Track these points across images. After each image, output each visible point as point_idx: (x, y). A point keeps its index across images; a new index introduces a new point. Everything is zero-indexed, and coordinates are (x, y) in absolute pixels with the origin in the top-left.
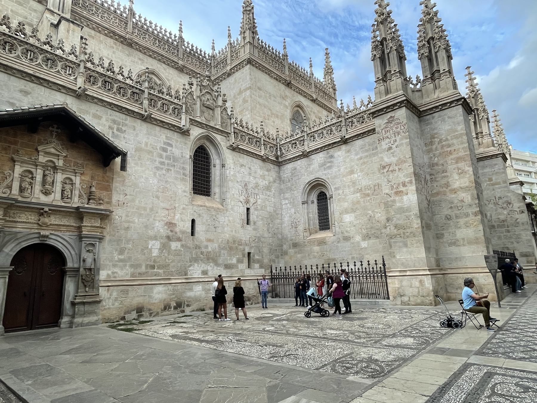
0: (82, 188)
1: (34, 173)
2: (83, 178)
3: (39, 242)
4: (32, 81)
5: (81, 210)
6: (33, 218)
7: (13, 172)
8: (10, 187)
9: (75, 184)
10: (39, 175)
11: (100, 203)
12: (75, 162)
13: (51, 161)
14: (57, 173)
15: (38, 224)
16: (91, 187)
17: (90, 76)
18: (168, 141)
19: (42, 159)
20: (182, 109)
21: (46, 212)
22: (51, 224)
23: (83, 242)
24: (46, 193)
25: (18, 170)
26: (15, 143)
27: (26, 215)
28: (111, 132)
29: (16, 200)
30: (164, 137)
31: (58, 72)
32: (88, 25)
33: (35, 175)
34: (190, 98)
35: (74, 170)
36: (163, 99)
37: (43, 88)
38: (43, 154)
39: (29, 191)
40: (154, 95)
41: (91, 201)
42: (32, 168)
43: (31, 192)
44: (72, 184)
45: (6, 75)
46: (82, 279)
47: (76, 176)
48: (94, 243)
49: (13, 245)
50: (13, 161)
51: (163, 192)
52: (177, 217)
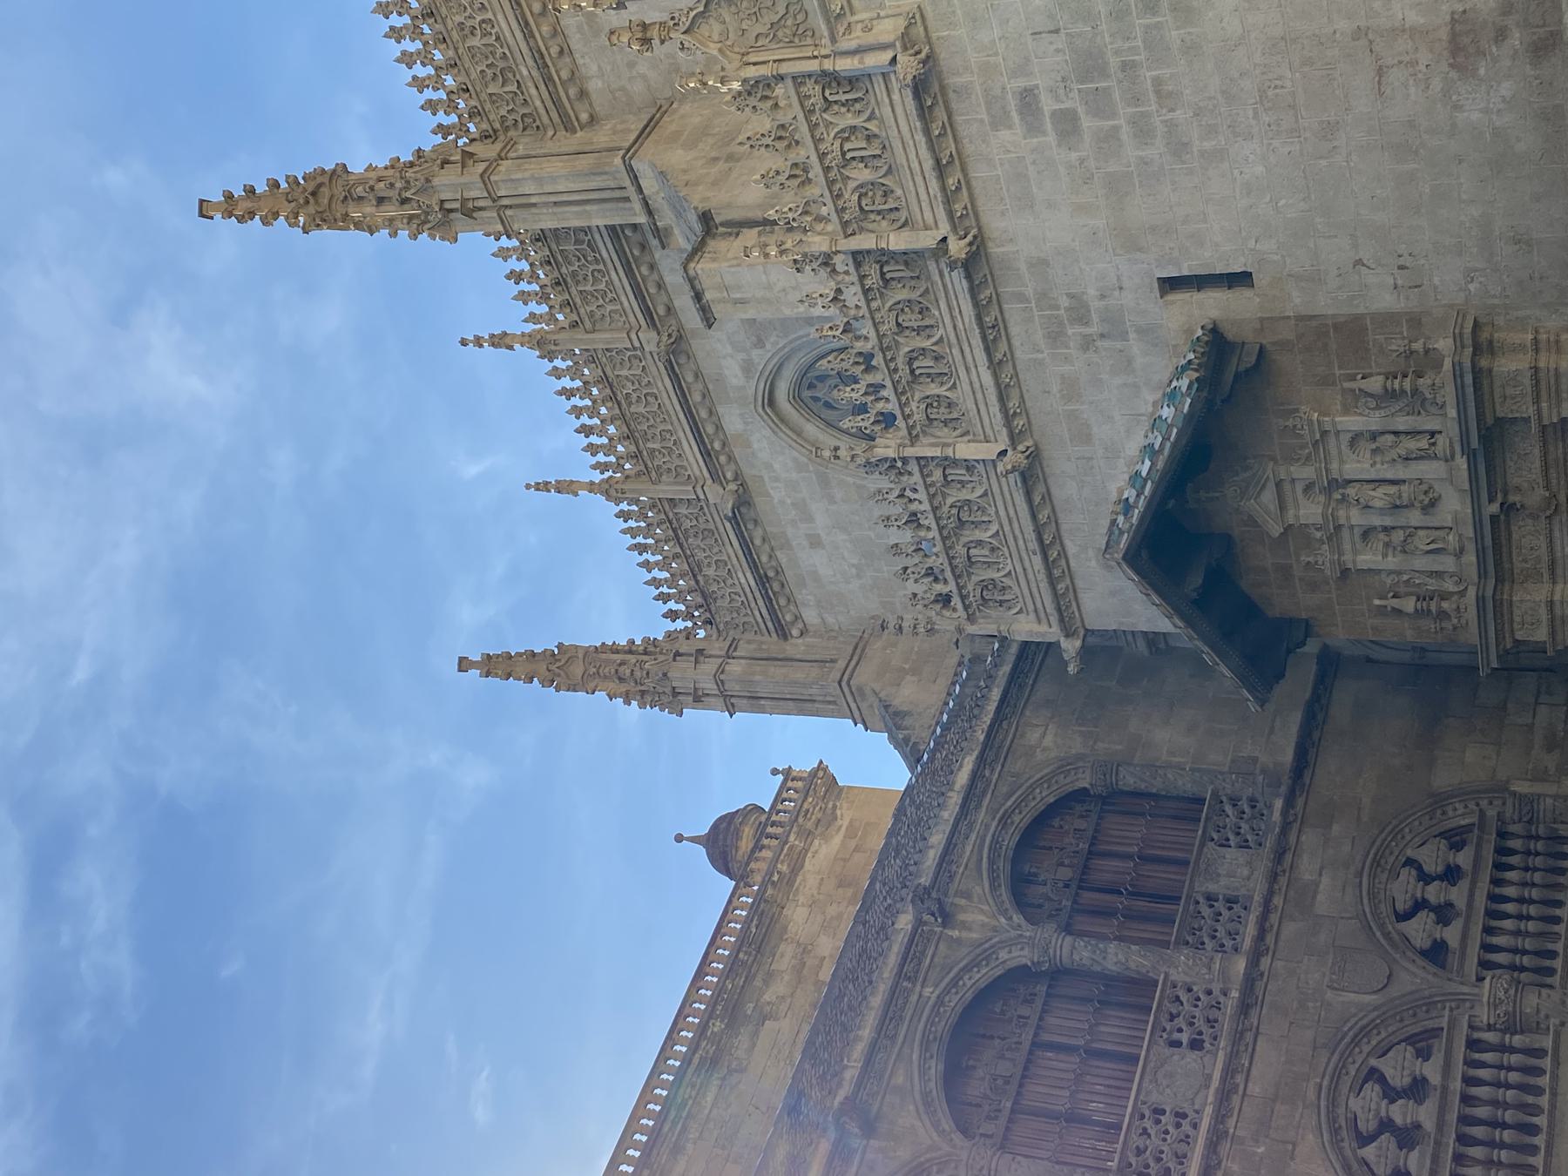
0: (1378, 408)
4: (1063, 553)
5: (1475, 444)
8: (1438, 574)
11: (1427, 351)
13: (1309, 488)
17: (930, 420)
18: (1014, 115)
19: (1309, 511)
20: (810, 76)
22: (1547, 487)
24: (1431, 505)
25: (1368, 558)
28: (1106, 343)
30: (1005, 135)
31: (985, 494)
32: (561, 52)
34: (717, 28)
36: (827, 170)
37: (1064, 527)
40: (840, 211)
44: (1374, 436)
45: (1080, 595)
47: (1338, 433)
50: (1345, 572)
51: (1292, 107)
52: (1414, 18)
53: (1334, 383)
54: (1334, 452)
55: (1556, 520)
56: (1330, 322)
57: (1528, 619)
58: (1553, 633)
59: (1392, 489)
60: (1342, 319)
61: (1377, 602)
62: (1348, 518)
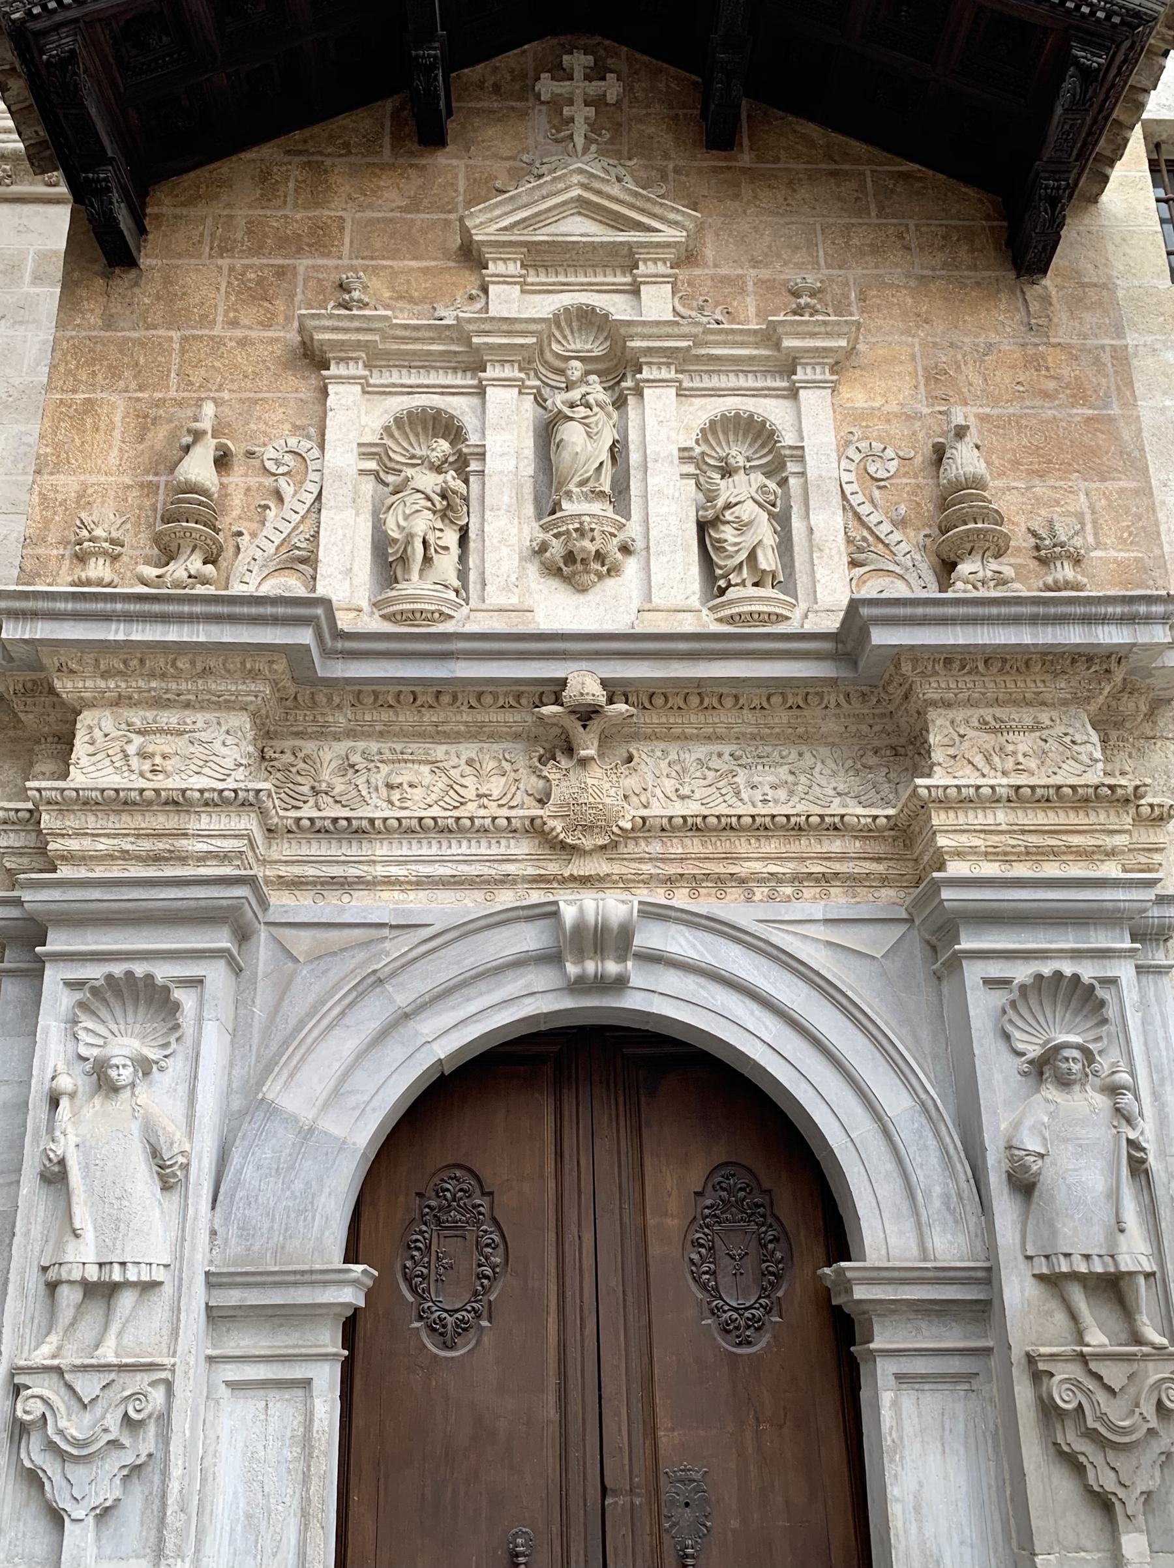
1: (470, 422)
2: (856, 396)
3: (567, 1003)
5: (881, 637)
6: (496, 786)
7: (322, 447)
8: (304, 559)
9: (801, 459)
10: (504, 427)
12: (768, 287)
13: (587, 319)
14: (639, 393)
15: (535, 829)
16: (939, 454)
21: (587, 714)
22: (644, 827)
23: (974, 972)
26: (320, 239)
27: (436, 766)
29: (313, 611)
33: (473, 439)
35: (770, 336)
38: (514, 268)
39: (446, 565)
41: (964, 568)
42: (445, 391)
43: (463, 575)
46: (1049, 1411)
47: (793, 393)
48: (1088, 971)
49: (344, 1044)
50: (312, 358)
53: (933, 399)
54: (715, 382)
55: (522, 847)
56: (1115, 411)
57: (159, 745)
58: (119, 803)
59: (607, 488)
60: (1126, 435)
61: (209, 409)
62: (506, 383)
